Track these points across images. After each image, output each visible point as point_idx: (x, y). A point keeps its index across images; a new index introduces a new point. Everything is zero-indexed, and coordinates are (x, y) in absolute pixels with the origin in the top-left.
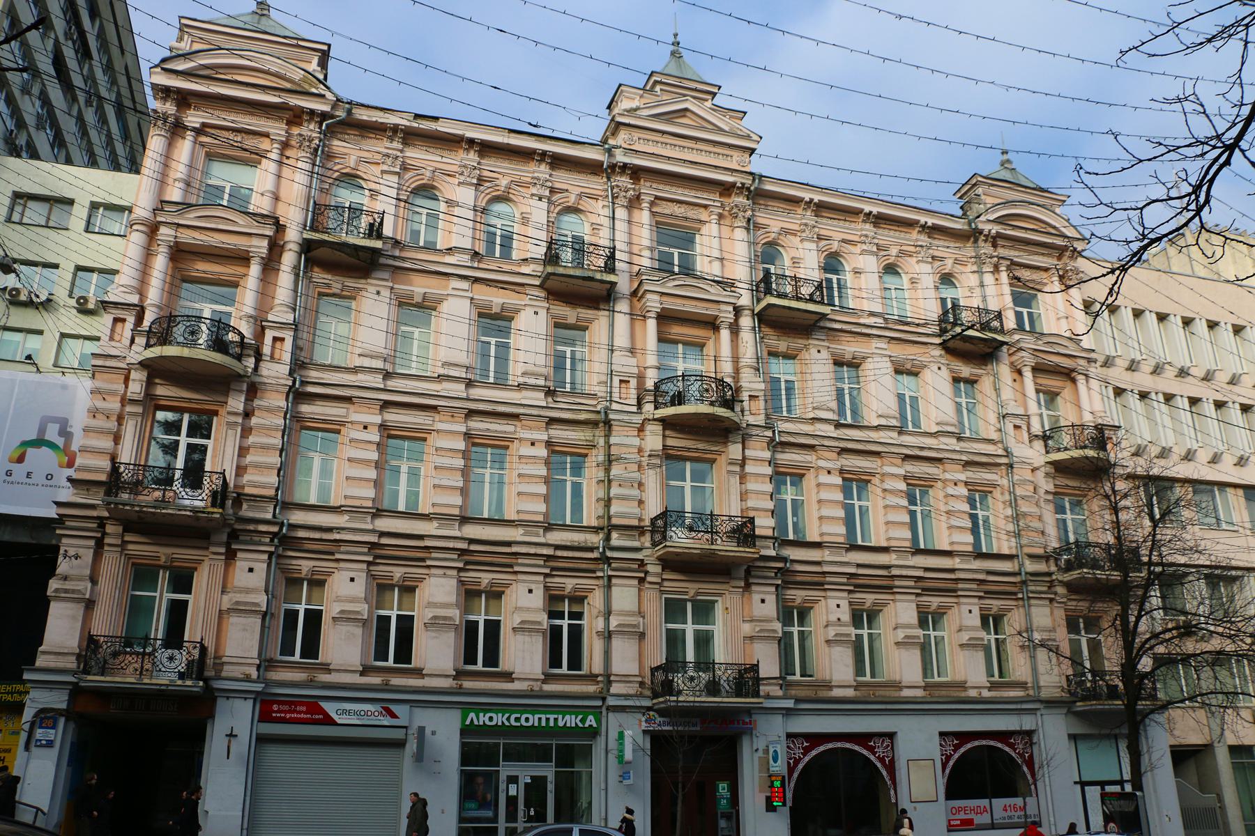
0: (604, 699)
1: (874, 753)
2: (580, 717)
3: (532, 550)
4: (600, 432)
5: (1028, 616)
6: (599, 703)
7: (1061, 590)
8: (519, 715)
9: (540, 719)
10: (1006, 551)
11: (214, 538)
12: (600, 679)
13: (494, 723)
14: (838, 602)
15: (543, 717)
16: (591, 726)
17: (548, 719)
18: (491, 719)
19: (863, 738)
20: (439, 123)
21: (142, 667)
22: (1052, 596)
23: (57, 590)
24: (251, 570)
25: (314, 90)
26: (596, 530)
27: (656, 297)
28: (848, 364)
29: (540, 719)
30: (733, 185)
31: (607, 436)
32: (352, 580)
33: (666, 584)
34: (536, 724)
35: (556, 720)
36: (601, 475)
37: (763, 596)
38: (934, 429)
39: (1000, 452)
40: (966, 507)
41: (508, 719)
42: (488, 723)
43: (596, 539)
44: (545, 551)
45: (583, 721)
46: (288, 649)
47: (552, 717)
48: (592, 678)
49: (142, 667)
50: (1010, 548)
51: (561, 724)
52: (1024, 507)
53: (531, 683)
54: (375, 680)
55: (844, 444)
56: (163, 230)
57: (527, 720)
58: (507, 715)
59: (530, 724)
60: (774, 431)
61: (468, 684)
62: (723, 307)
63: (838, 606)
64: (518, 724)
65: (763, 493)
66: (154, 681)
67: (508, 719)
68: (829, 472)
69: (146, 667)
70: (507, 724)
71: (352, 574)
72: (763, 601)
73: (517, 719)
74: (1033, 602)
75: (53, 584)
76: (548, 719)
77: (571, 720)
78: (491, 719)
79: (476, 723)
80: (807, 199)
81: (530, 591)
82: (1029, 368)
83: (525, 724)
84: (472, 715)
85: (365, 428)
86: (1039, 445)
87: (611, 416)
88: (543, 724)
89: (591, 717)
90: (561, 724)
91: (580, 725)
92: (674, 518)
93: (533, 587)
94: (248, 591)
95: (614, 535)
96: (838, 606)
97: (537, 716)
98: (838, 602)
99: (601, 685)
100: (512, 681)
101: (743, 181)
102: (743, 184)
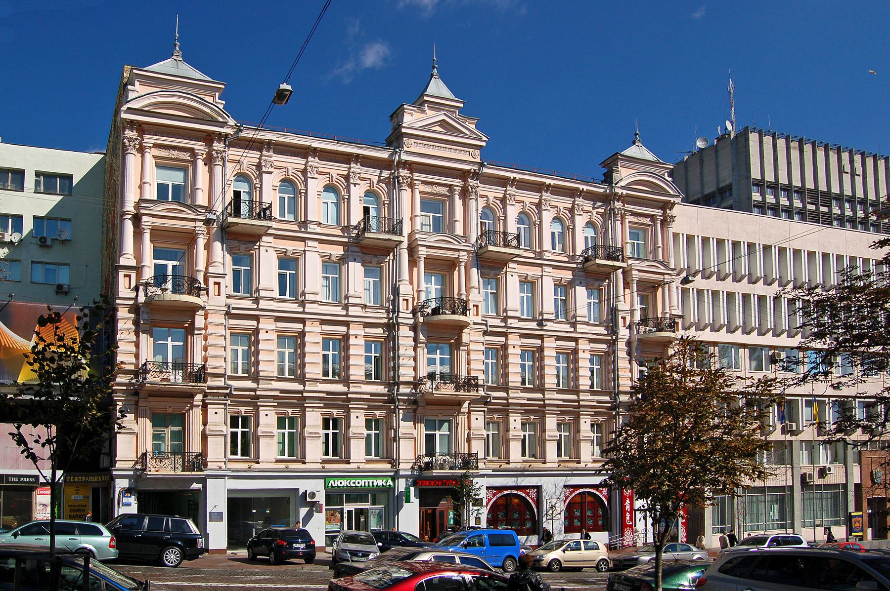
2: (385, 480)
8: (354, 481)
9: (365, 482)
11: (196, 398)
13: (342, 485)
14: (515, 418)
15: (367, 481)
16: (390, 485)
17: (369, 482)
18: (341, 483)
21: (175, 467)
24: (216, 413)
25: (220, 119)
27: (424, 249)
29: (365, 482)
30: (469, 171)
32: (267, 415)
34: (363, 485)
35: (373, 482)
37: (477, 417)
40: (589, 365)
41: (349, 483)
42: (340, 485)
46: (234, 452)
47: (371, 481)
49: (175, 467)
51: (375, 484)
53: (359, 464)
54: (282, 466)
56: (144, 218)
57: (359, 483)
58: (349, 481)
59: (360, 485)
60: (486, 325)
61: (327, 466)
63: (515, 420)
65: (479, 360)
67: (349, 483)
68: (514, 347)
69: (177, 466)
70: (349, 485)
71: (267, 413)
72: (477, 419)
76: (369, 482)
77: (380, 482)
78: (341, 483)
79: (334, 485)
80: (512, 178)
83: (358, 485)
84: (332, 482)
87: (400, 320)
88: (367, 485)
89: (390, 480)
90: (375, 484)
91: (385, 485)
93: (358, 415)
94: (216, 424)
95: (401, 386)
96: (515, 420)
97: (363, 481)
98: (515, 418)
101: (475, 168)
102: (475, 170)
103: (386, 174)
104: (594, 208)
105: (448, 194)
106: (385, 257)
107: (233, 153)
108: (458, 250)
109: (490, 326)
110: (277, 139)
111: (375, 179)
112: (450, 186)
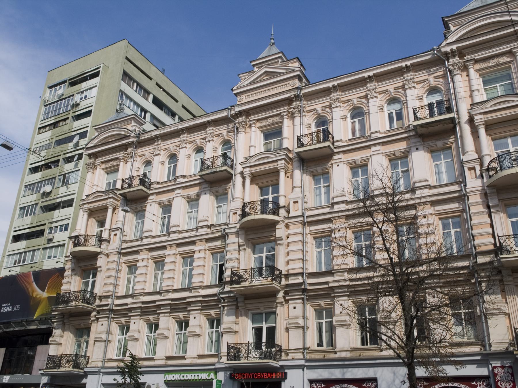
3: (194, 299)
17: (195, 376)
23: (51, 341)
27: (248, 169)
33: (248, 306)
37: (294, 305)
41: (180, 376)
44: (199, 299)
45: (209, 376)
47: (196, 375)
62: (279, 162)
64: (183, 379)
66: (59, 370)
67: (180, 376)
73: (183, 376)
75: (51, 339)
81: (195, 318)
85: (143, 261)
92: (249, 273)
93: (196, 316)
97: (191, 375)
100: (185, 359)
101: (294, 93)
102: (294, 95)
103: (231, 125)
104: (429, 75)
105: (280, 120)
106: (226, 185)
107: (140, 151)
108: (276, 161)
109: (307, 217)
110: (159, 133)
111: (224, 133)
112: (280, 114)
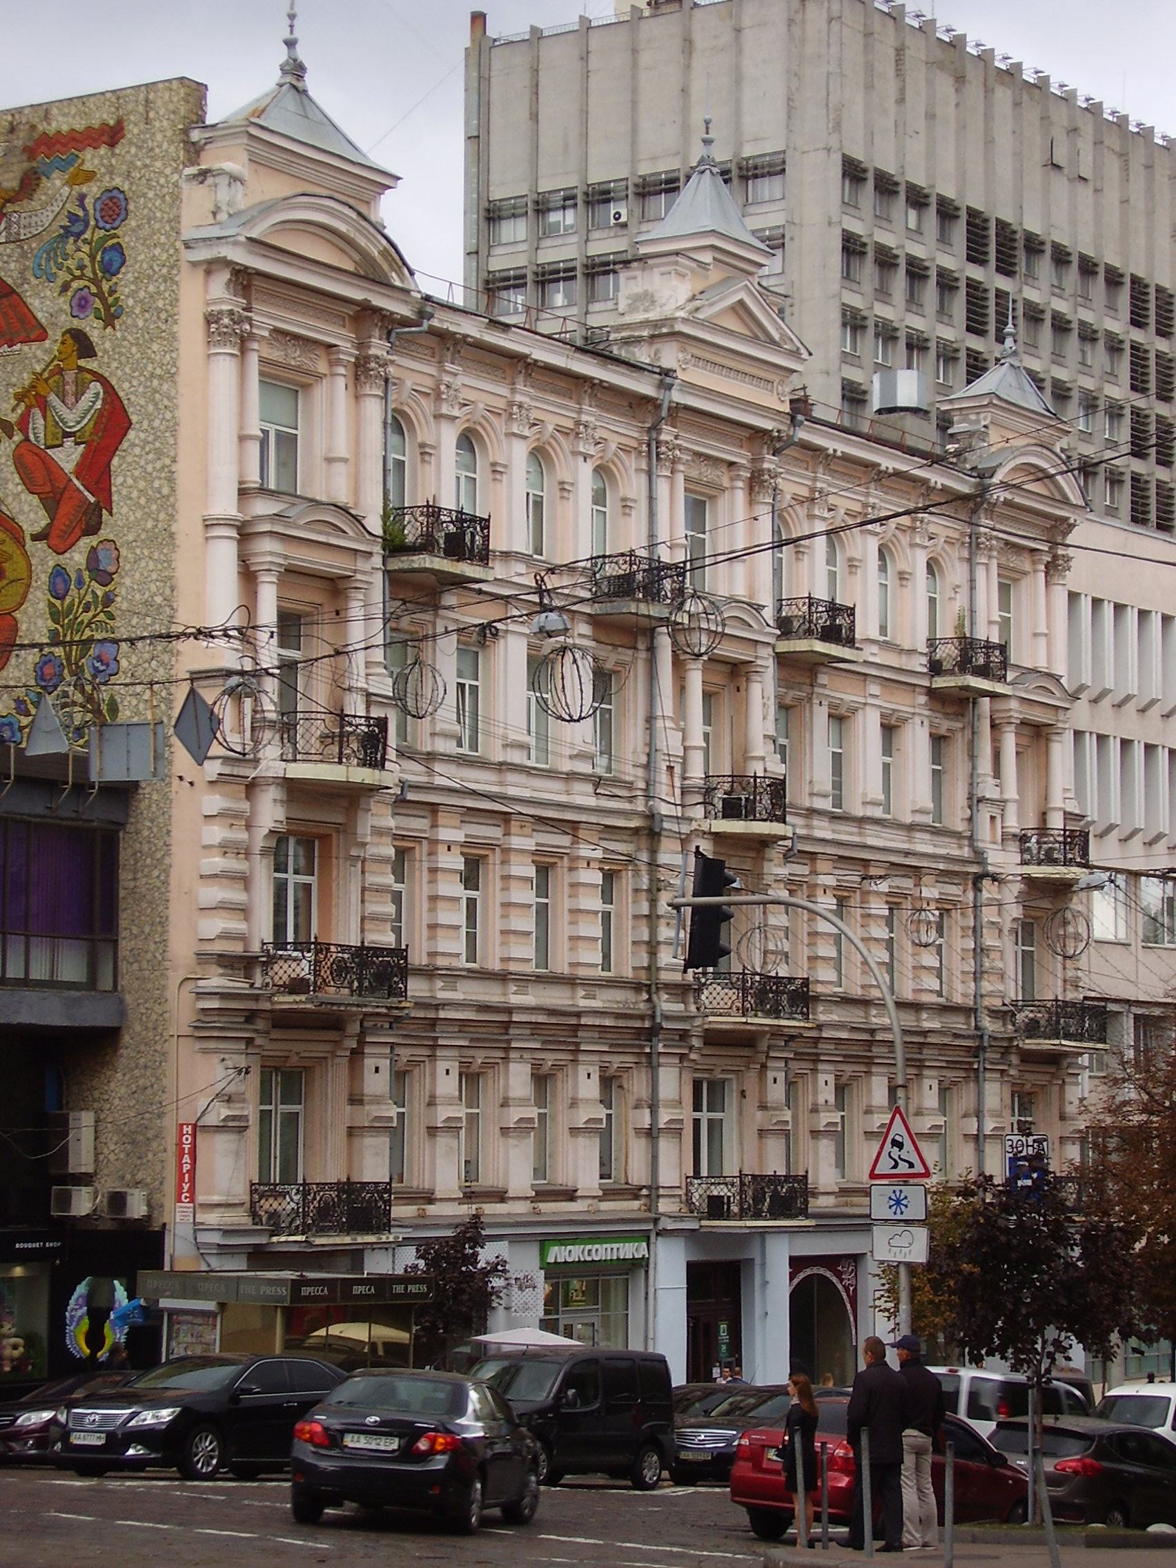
0: (656, 1221)
1: (841, 1281)
4: (644, 843)
5: (980, 1095)
6: (651, 1227)
7: (1015, 1059)
10: (958, 999)
12: (644, 1192)
19: (831, 1261)
20: (511, 336)
22: (1005, 1067)
26: (637, 987)
28: (840, 718)
31: (653, 852)
36: (645, 909)
38: (908, 819)
39: (966, 852)
43: (638, 1003)
48: (634, 1193)
50: (965, 995)
52: (989, 940)
55: (841, 852)
61: (545, 1207)
74: (988, 1075)
82: (1012, 728)
86: (1014, 846)
99: (643, 1201)
